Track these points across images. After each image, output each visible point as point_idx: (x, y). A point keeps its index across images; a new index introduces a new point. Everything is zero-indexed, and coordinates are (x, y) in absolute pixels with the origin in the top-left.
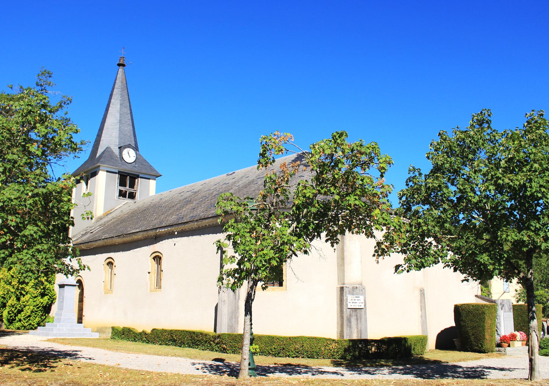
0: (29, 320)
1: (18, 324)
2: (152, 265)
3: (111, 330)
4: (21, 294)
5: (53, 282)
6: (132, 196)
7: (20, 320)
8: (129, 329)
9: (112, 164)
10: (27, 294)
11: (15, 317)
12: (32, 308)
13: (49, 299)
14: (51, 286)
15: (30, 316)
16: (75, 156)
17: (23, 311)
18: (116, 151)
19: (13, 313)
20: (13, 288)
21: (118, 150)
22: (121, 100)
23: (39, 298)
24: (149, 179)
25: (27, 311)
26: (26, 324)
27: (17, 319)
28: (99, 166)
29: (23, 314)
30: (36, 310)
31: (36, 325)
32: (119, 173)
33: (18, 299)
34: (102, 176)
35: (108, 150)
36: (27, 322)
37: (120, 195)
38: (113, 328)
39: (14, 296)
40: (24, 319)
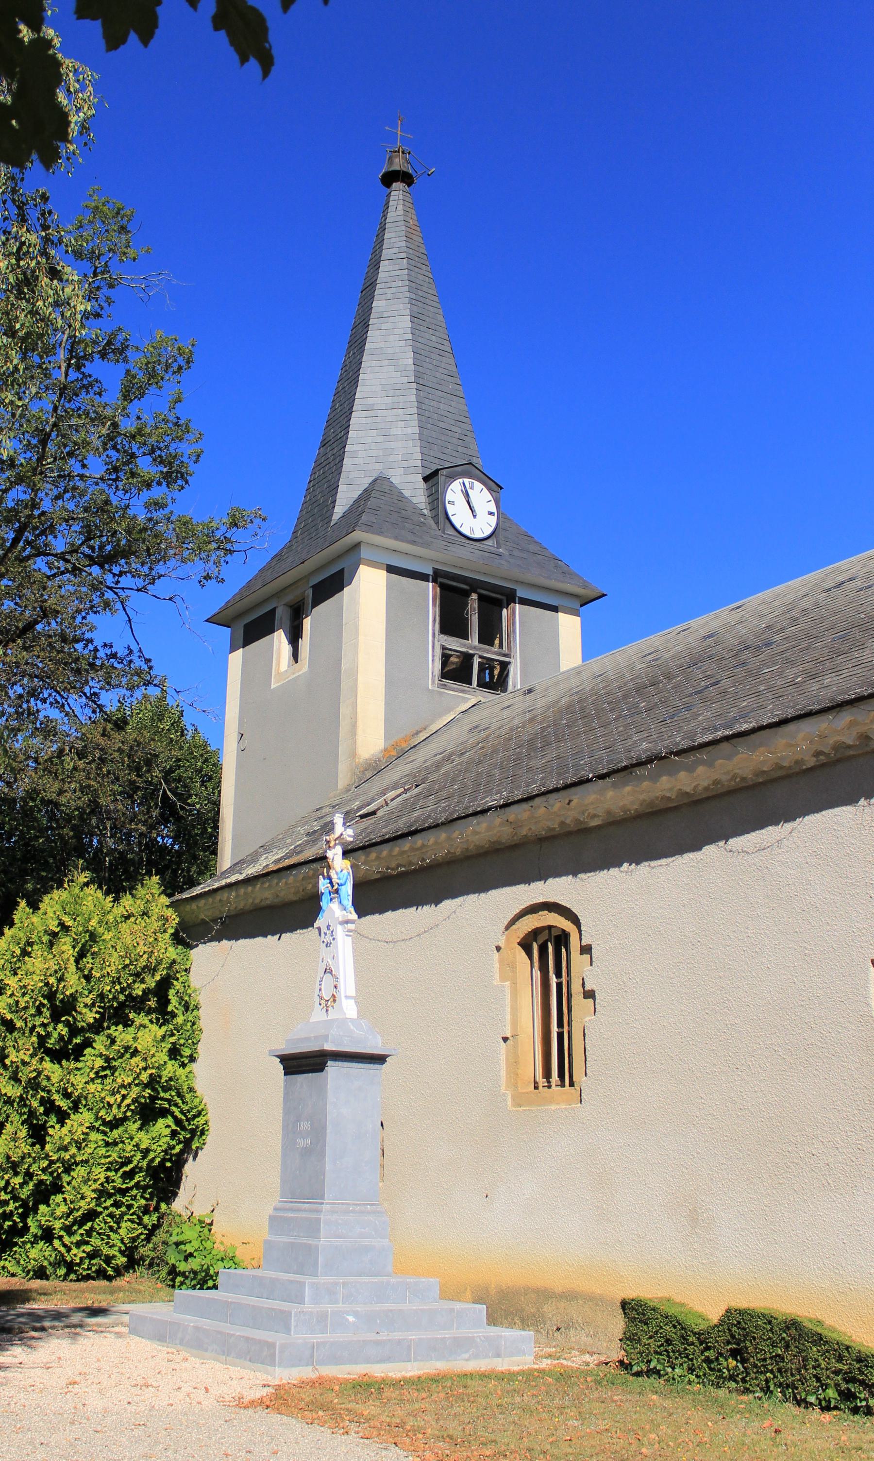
0: (89, 1233)
1: (39, 1253)
2: (514, 996)
3: (618, 1324)
4: (50, 1107)
5: (187, 1052)
6: (495, 679)
7: (48, 1235)
8: (793, 1325)
9: (411, 537)
10: (75, 1108)
11: (24, 1217)
12: (100, 1174)
13: (174, 1134)
14: (181, 1072)
15: (91, 1215)
16: (208, 577)
17: (57, 1188)
18: (415, 492)
19: (15, 1198)
20: (15, 1078)
21: (422, 484)
22: (411, 301)
23: (133, 1126)
24: (555, 609)
25: (81, 1189)
26: (77, 1254)
27: (34, 1230)
28: (357, 546)
29: (59, 1204)
30: (119, 1183)
31: (122, 1260)
32: (437, 576)
33: (38, 1134)
34: (370, 586)
35: (378, 489)
36: (78, 1244)
37: (445, 675)
38: (632, 1309)
39: (15, 1118)
40: (68, 1230)
